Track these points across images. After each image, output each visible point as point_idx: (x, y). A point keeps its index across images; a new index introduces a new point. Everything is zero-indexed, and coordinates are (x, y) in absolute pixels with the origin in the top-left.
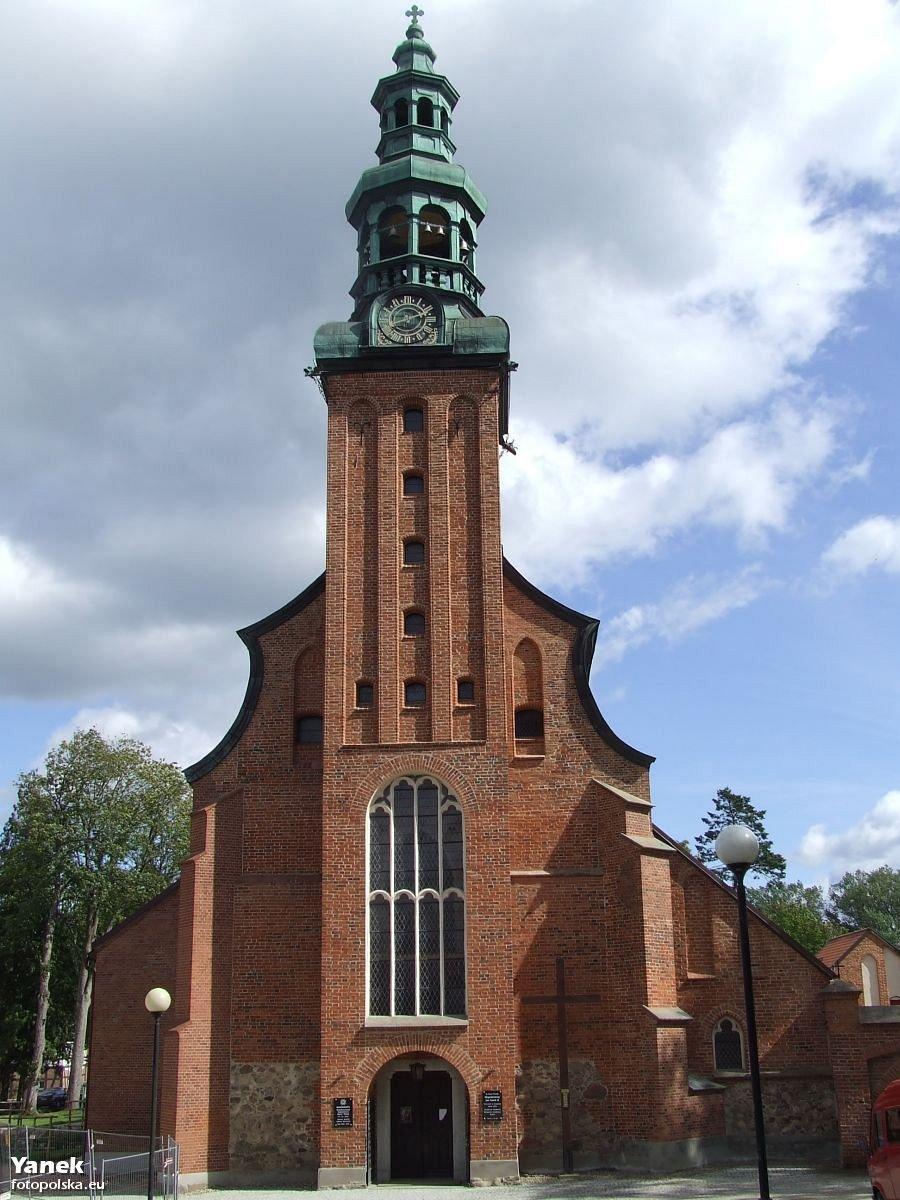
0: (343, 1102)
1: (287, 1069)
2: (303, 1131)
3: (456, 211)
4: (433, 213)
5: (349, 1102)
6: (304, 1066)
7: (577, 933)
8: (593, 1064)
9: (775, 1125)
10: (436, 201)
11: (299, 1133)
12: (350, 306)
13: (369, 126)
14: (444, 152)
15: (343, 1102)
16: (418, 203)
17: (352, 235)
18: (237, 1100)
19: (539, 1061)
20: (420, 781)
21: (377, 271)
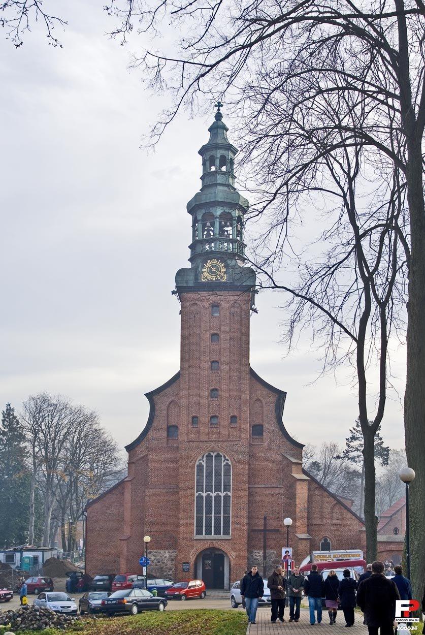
1: (165, 552)
2: (171, 573)
7: (272, 507)
8: (275, 552)
11: (169, 573)
16: (218, 211)
19: (256, 551)
20: (216, 454)
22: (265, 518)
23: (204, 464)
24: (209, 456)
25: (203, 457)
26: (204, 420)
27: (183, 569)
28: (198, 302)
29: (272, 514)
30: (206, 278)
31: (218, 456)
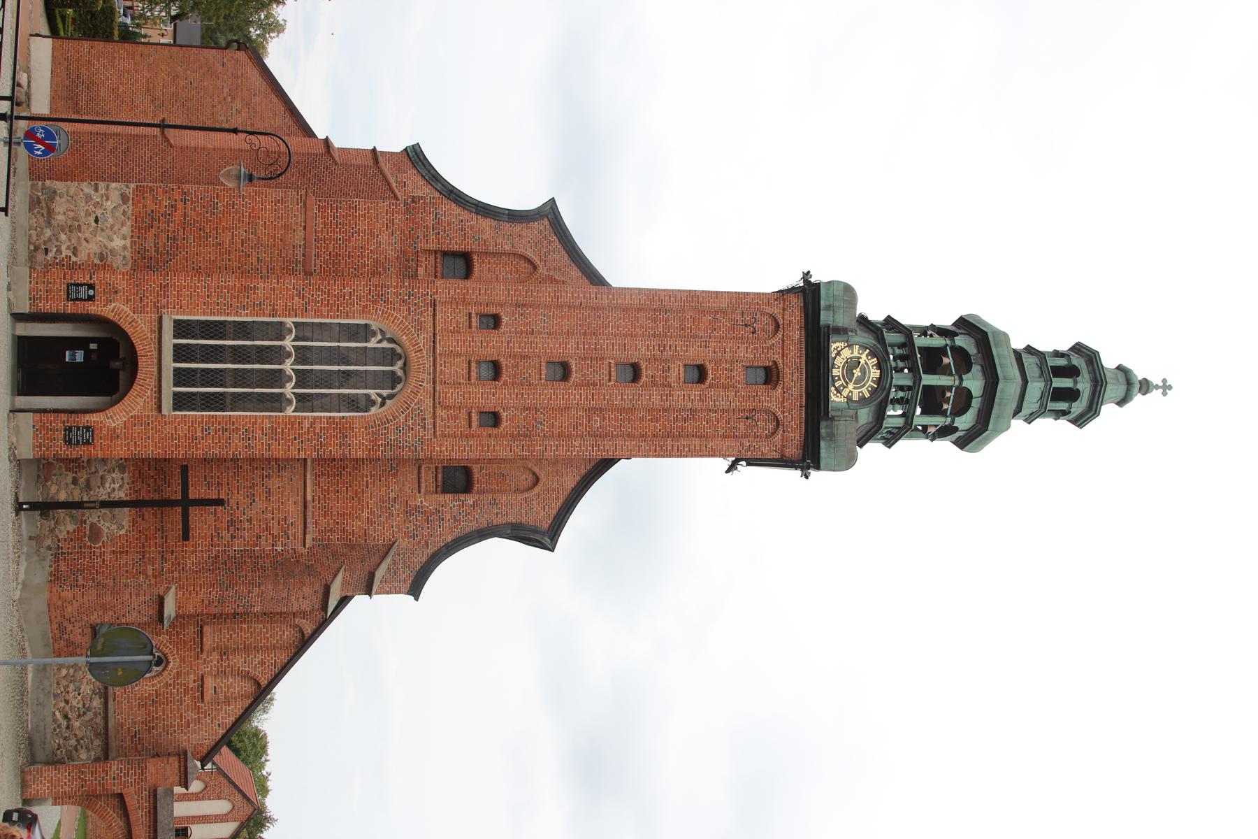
0: (91, 292)
1: (124, 238)
2: (65, 252)
3: (965, 422)
4: (964, 399)
5: (91, 298)
6: (128, 254)
7: (250, 520)
8: (123, 532)
9: (62, 704)
10: (976, 404)
11: (63, 248)
12: (876, 316)
13: (1054, 340)
14: (1026, 411)
15: (91, 292)
17: (947, 320)
18: (96, 190)
20: (400, 373)
21: (908, 343)
22: (220, 502)
23: (372, 344)
25: (391, 340)
27: (77, 285)
28: (780, 335)
29: (231, 523)
30: (838, 354)
31: (394, 380)
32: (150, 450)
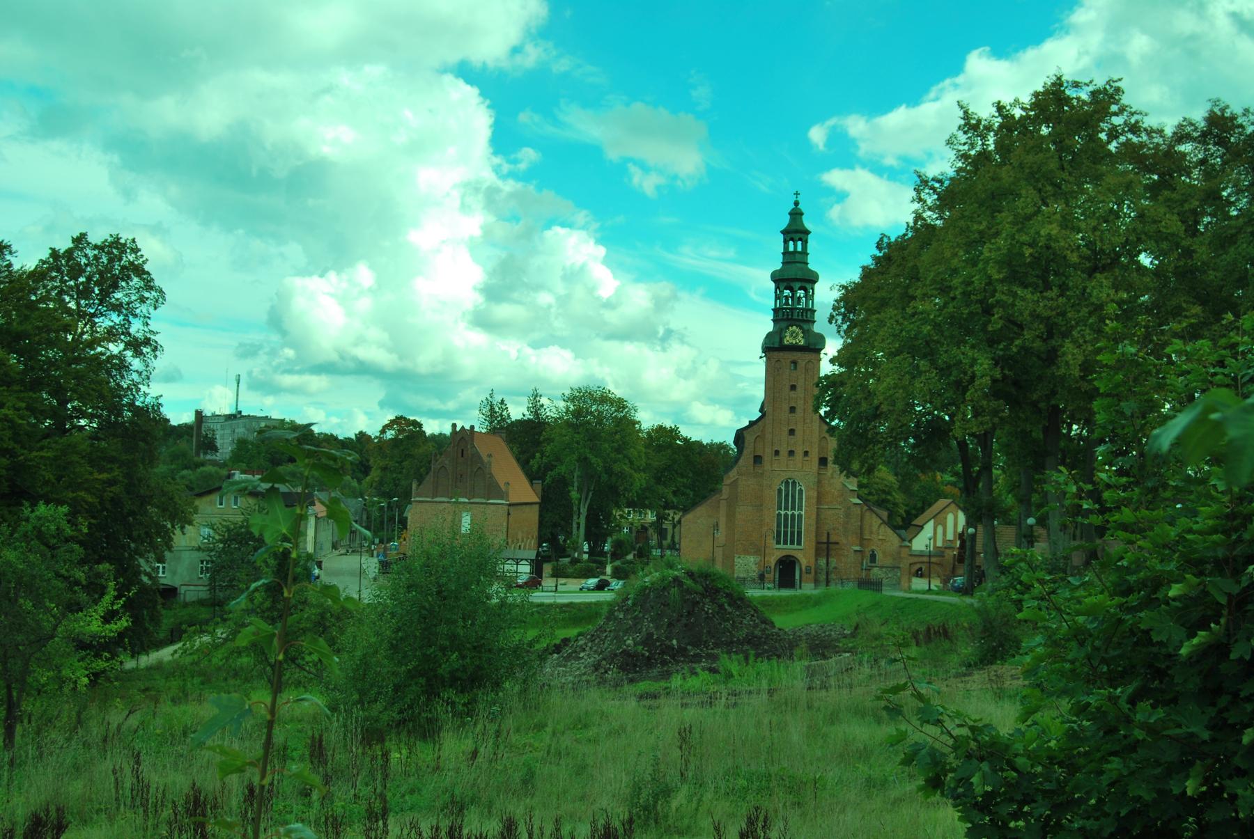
24: (787, 483)
26: (784, 453)
32: (812, 552)
